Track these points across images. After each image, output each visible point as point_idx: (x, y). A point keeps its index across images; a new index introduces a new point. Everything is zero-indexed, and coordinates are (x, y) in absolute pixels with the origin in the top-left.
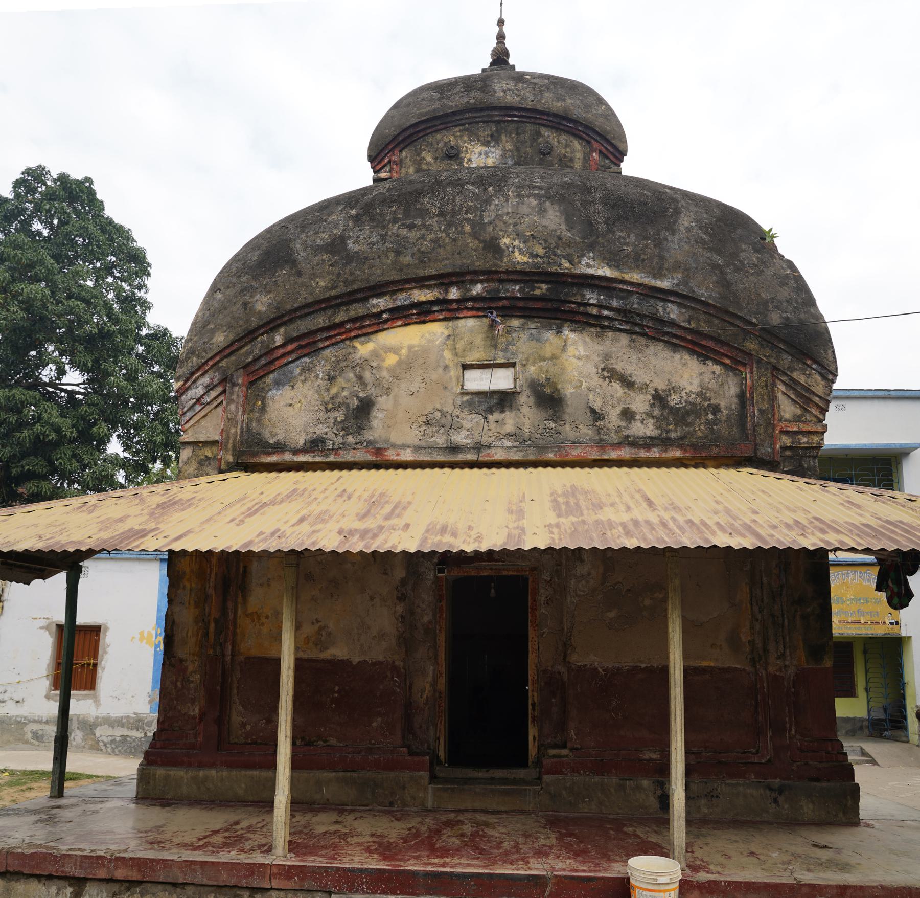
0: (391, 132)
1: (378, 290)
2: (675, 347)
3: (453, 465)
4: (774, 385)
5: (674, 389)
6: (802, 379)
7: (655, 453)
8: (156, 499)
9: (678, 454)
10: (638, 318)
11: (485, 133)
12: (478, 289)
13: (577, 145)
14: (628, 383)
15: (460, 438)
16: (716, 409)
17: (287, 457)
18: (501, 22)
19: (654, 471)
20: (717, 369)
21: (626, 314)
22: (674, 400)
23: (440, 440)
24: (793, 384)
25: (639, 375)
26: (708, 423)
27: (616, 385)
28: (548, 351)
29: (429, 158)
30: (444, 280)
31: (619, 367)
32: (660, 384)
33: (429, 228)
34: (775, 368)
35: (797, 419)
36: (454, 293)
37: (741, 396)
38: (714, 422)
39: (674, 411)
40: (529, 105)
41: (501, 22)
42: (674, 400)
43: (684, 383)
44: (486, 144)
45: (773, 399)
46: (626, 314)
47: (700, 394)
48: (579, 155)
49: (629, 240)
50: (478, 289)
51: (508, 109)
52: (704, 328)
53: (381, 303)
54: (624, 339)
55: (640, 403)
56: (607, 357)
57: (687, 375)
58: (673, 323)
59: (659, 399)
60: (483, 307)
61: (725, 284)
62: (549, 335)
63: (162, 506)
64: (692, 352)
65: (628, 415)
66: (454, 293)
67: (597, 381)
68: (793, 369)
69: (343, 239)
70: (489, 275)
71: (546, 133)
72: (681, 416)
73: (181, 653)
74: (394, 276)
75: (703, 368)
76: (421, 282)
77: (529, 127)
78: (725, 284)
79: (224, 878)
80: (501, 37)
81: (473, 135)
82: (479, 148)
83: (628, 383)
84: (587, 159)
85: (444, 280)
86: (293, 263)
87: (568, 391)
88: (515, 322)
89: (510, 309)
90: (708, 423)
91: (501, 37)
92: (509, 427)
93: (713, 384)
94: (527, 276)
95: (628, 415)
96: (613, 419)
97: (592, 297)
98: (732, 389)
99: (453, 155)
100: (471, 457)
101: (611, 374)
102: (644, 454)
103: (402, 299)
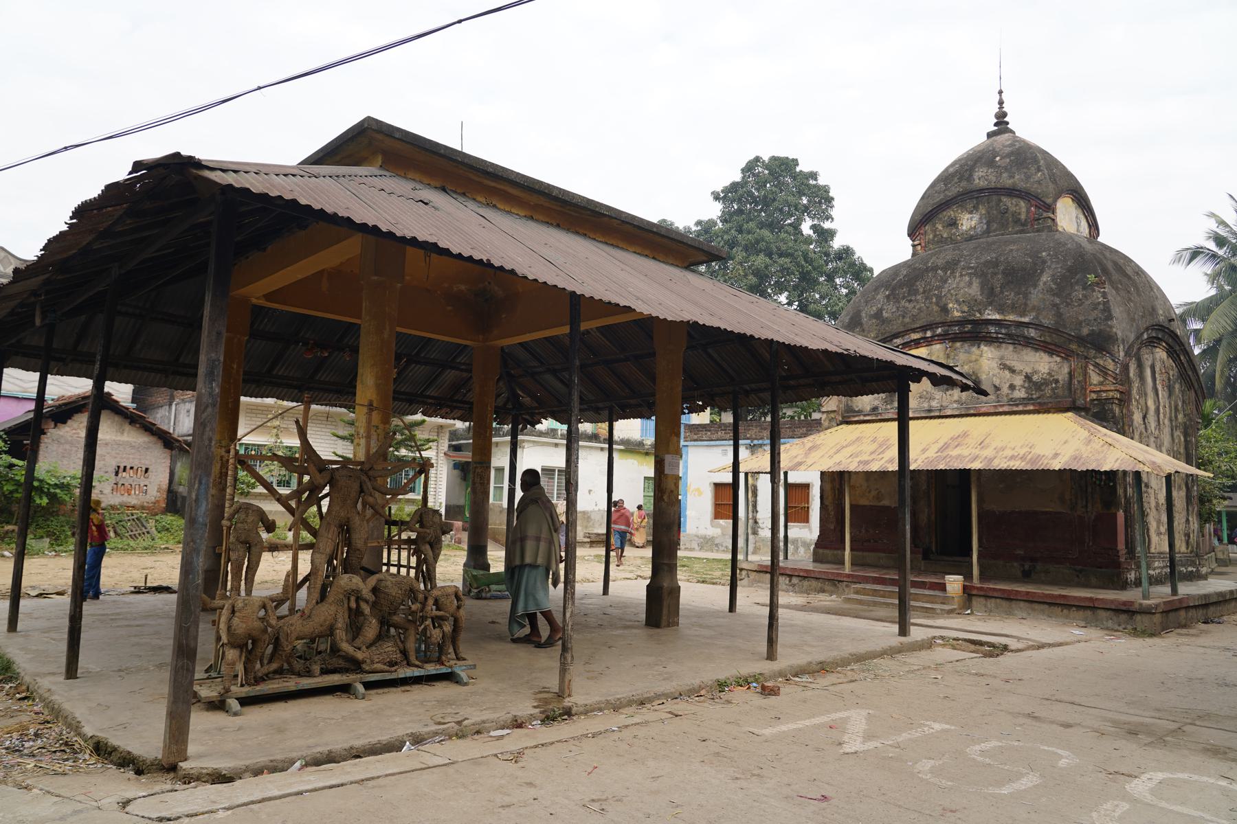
0: (918, 218)
1: (896, 336)
2: (1036, 350)
3: (931, 418)
4: (1086, 367)
5: (1036, 372)
6: (1101, 363)
7: (1021, 408)
8: (810, 445)
9: (1032, 408)
10: (1016, 337)
11: (970, 206)
12: (939, 331)
13: (1022, 204)
14: (1012, 371)
15: (934, 404)
16: (1057, 381)
17: (862, 418)
18: (1000, 92)
19: (1022, 416)
20: (1058, 359)
21: (1010, 336)
22: (1035, 378)
23: (926, 405)
24: (1097, 365)
25: (1018, 366)
26: (1053, 389)
27: (1007, 372)
28: (973, 358)
29: (940, 227)
30: (924, 328)
31: (1008, 363)
32: (1029, 370)
33: (917, 301)
34: (1086, 358)
35: (1101, 383)
36: (929, 334)
37: (1070, 373)
38: (1056, 388)
39: (1035, 384)
40: (993, 185)
41: (1000, 92)
42: (1035, 378)
43: (1041, 368)
44: (971, 212)
45: (1085, 374)
46: (1010, 336)
47: (1049, 374)
48: (1024, 210)
49: (1010, 296)
50: (939, 331)
51: (981, 190)
52: (1048, 340)
53: (898, 341)
54: (1011, 347)
55: (1018, 381)
56: (1002, 358)
57: (1042, 364)
58: (1032, 338)
59: (1028, 378)
60: (943, 338)
61: (1059, 315)
62: (974, 349)
63: (810, 449)
64: (1045, 352)
65: (1012, 387)
66: (929, 334)
67: (997, 371)
68: (1095, 357)
69: (880, 311)
70: (943, 324)
71: (1004, 199)
72: (1038, 386)
73: (827, 503)
74: (902, 329)
75: (1051, 360)
76: (914, 330)
77: (995, 198)
78: (1059, 315)
79: (831, 577)
80: (1001, 103)
81: (963, 208)
82: (968, 216)
83: (1012, 371)
84: (1028, 211)
85: (924, 328)
86: (861, 324)
87: (983, 377)
88: (958, 344)
89: (954, 339)
90: (1053, 389)
91: (1001, 103)
92: (956, 398)
93: (1055, 368)
94: (961, 322)
95: (1012, 387)
96: (1005, 390)
97: (992, 329)
98: (1066, 370)
99: (953, 223)
100: (937, 414)
101: (1004, 367)
102: (1015, 409)
103: (907, 339)
